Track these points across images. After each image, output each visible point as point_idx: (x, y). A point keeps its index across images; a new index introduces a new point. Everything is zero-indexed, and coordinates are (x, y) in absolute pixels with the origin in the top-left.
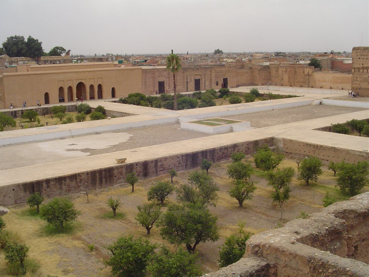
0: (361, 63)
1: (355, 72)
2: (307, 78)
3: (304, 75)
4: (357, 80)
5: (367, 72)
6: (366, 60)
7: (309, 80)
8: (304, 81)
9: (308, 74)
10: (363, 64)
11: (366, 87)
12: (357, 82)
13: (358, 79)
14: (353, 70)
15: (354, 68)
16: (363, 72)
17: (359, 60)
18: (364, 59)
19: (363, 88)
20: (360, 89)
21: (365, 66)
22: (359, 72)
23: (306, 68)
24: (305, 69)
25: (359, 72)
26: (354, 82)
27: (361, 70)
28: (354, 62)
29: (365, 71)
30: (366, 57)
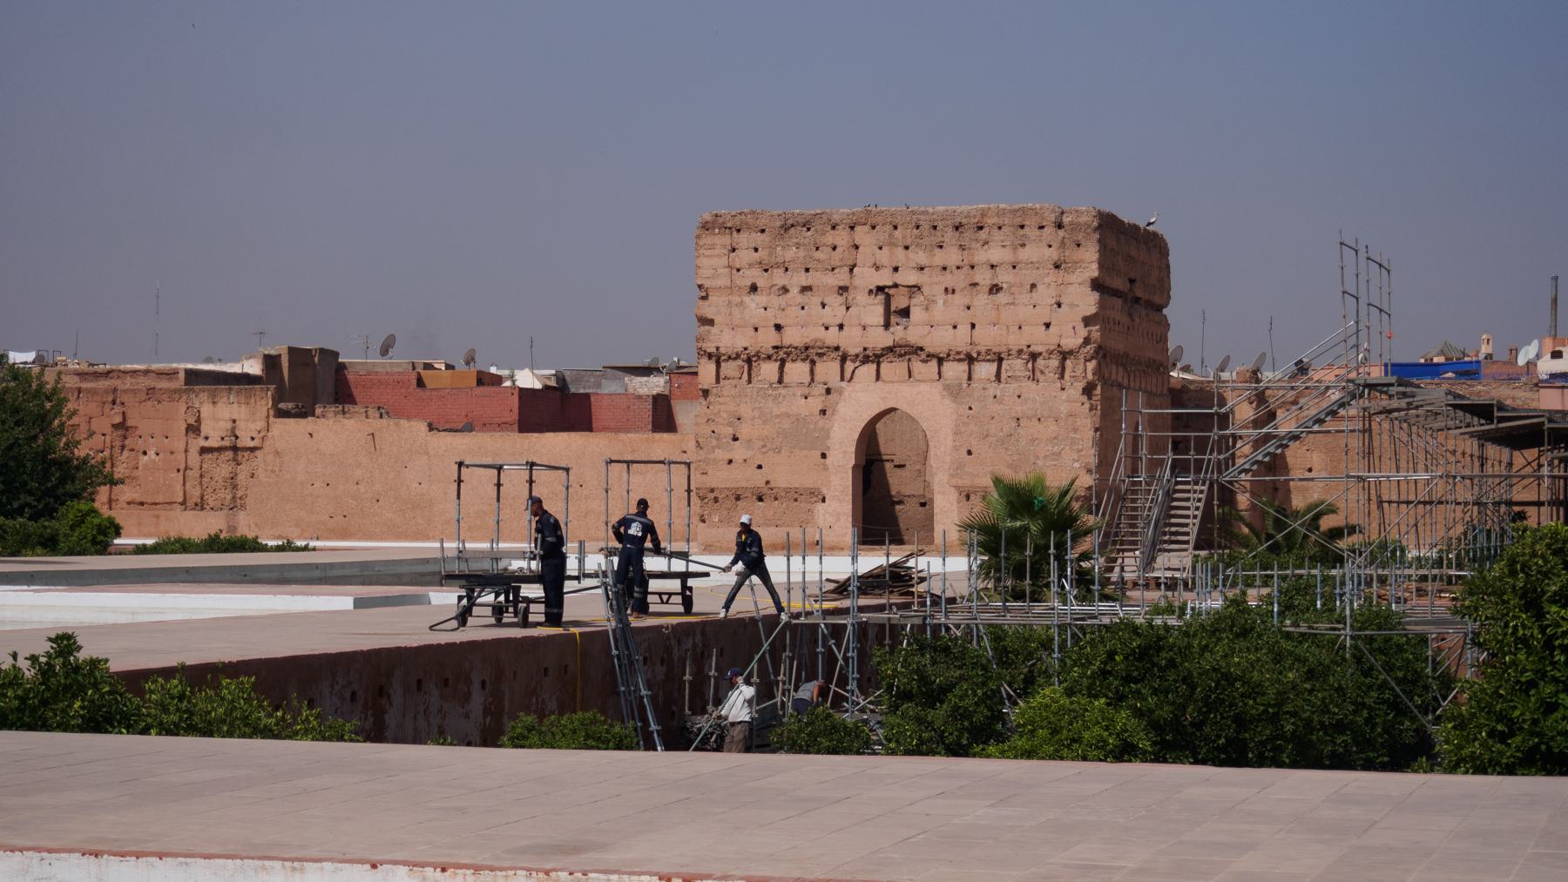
0: (773, 317)
1: (718, 381)
2: (221, 468)
3: (194, 457)
4: (735, 439)
5: (807, 379)
6: (800, 299)
7: (235, 487)
8: (195, 493)
9: (227, 443)
10: (778, 327)
12: (738, 452)
13: (745, 431)
14: (707, 370)
15: (717, 358)
16: (780, 381)
17: (747, 299)
18: (785, 290)
19: (787, 490)
20: (760, 499)
21: (793, 337)
22: (750, 381)
24: (206, 410)
25: (750, 381)
27: (768, 370)
29: (797, 371)
30: (803, 279)
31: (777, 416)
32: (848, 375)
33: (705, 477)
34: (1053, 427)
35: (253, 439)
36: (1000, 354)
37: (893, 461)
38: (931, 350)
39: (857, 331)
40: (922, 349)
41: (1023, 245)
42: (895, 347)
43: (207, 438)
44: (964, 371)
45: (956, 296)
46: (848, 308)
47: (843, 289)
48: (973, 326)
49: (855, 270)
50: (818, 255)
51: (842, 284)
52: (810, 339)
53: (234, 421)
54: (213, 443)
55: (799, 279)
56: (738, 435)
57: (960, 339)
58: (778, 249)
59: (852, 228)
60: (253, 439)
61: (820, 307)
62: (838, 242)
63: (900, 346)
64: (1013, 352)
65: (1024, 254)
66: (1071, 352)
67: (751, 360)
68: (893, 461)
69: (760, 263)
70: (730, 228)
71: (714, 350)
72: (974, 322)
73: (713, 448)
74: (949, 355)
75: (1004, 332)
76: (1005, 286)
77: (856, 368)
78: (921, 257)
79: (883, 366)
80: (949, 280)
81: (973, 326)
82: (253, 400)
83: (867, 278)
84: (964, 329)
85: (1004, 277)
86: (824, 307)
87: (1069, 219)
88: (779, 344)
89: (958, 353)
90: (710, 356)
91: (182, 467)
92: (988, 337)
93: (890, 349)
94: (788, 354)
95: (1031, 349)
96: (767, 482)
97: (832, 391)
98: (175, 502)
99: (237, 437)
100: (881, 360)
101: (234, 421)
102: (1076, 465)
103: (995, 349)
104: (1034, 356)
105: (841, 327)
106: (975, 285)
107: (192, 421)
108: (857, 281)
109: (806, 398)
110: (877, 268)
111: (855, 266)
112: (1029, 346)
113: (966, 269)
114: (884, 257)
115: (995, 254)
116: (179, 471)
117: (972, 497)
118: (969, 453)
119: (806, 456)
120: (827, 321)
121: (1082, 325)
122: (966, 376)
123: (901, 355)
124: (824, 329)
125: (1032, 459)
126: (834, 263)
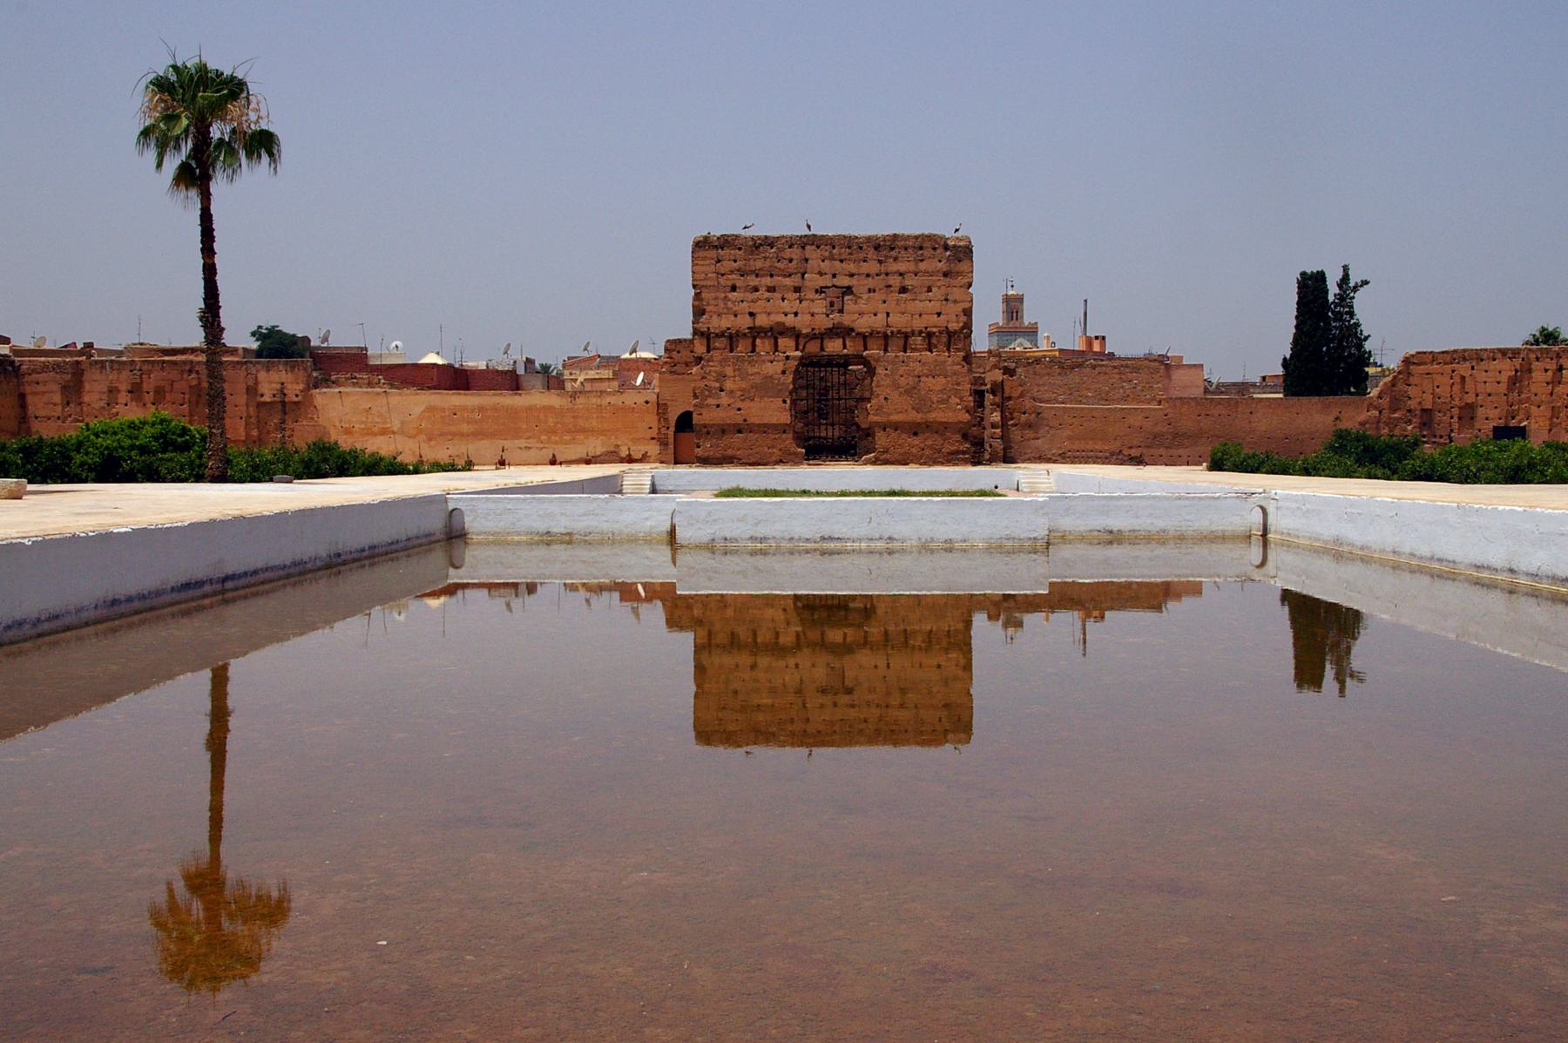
4: (722, 390)
6: (767, 295)
10: (751, 314)
11: (774, 421)
12: (724, 399)
13: (729, 385)
18: (756, 289)
19: (759, 425)
21: (762, 320)
23: (268, 371)
24: (262, 375)
26: (711, 401)
28: (708, 304)
29: (763, 345)
30: (768, 281)
31: (752, 375)
33: (700, 417)
34: (944, 381)
35: (297, 396)
36: (907, 333)
38: (860, 330)
39: (808, 317)
41: (922, 260)
43: (262, 395)
45: (876, 294)
46: (800, 302)
47: (797, 290)
48: (888, 314)
49: (806, 276)
50: (778, 265)
51: (796, 285)
53: (283, 384)
54: (267, 398)
55: (768, 281)
56: (724, 388)
57: (878, 322)
58: (752, 261)
59: (803, 248)
60: (297, 396)
62: (794, 256)
64: (917, 332)
65: (923, 266)
66: (955, 332)
67: (732, 338)
69: (738, 271)
70: (716, 246)
71: (706, 329)
73: (707, 397)
74: (871, 334)
75: (910, 319)
76: (910, 287)
77: (806, 342)
78: (852, 267)
79: (825, 342)
80: (870, 283)
81: (888, 314)
82: (296, 370)
83: (813, 281)
84: (881, 317)
85: (908, 282)
86: (783, 301)
87: (953, 243)
88: (752, 325)
89: (878, 333)
90: (702, 334)
91: (244, 415)
92: (898, 321)
93: (831, 329)
94: (759, 333)
95: (928, 329)
96: (745, 420)
98: (239, 440)
99: (285, 395)
101: (283, 384)
102: (959, 407)
103: (904, 330)
104: (930, 335)
105: (796, 314)
106: (890, 286)
107: (251, 383)
108: (807, 283)
110: (821, 274)
111: (805, 273)
112: (926, 328)
113: (883, 276)
114: (826, 266)
115: (902, 267)
116: (241, 418)
120: (787, 310)
121: (962, 314)
125: (930, 403)
126: (791, 271)
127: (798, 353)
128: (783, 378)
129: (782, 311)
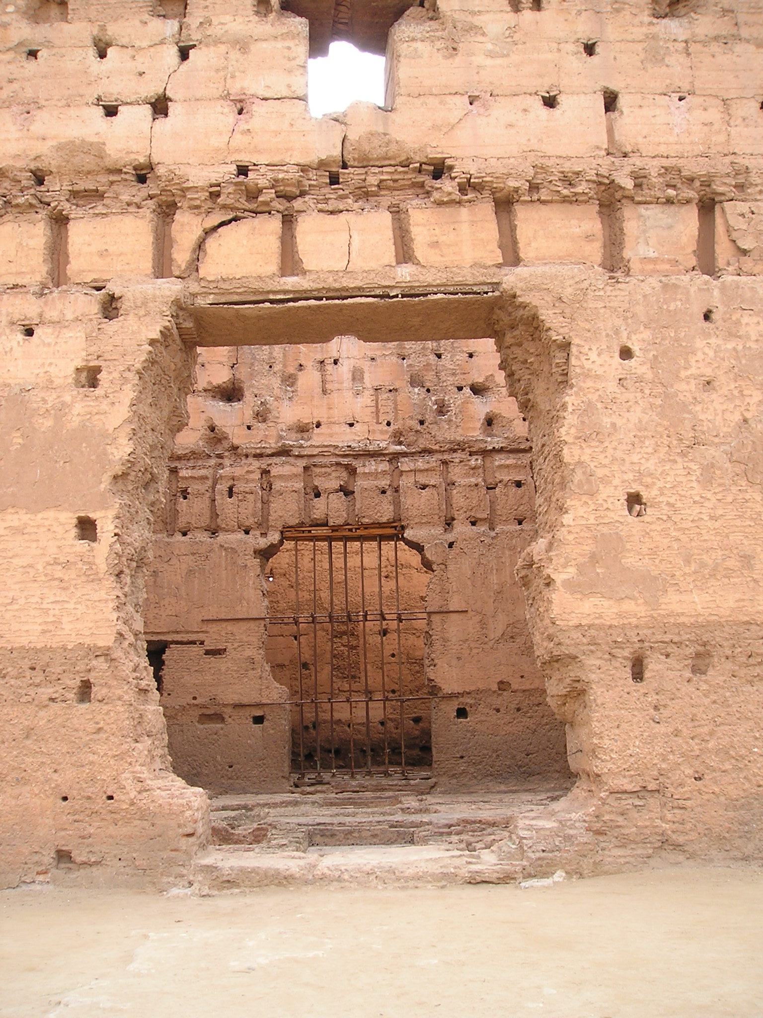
32: (181, 256)
37: (202, 643)
40: (439, 170)
42: (345, 166)
44: (589, 238)
46: (184, 54)
48: (611, 101)
52: (50, 143)
61: (92, 52)
63: (365, 163)
68: (202, 643)
72: (613, 87)
81: (611, 101)
86: (102, 55)
89: (568, 180)
97: (125, 305)
100: (298, 204)
103: (691, 167)
109: (29, 332)
117: (654, 666)
118: (634, 500)
119: (19, 531)
120: (113, 90)
122: (595, 251)
123: (364, 194)
124: (101, 111)
127: (170, 288)
128: (78, 408)
129: (92, 93)
